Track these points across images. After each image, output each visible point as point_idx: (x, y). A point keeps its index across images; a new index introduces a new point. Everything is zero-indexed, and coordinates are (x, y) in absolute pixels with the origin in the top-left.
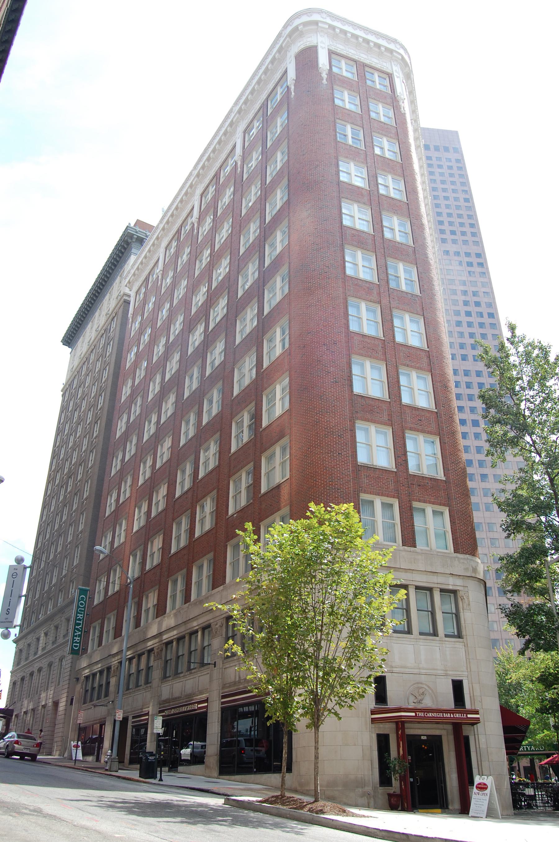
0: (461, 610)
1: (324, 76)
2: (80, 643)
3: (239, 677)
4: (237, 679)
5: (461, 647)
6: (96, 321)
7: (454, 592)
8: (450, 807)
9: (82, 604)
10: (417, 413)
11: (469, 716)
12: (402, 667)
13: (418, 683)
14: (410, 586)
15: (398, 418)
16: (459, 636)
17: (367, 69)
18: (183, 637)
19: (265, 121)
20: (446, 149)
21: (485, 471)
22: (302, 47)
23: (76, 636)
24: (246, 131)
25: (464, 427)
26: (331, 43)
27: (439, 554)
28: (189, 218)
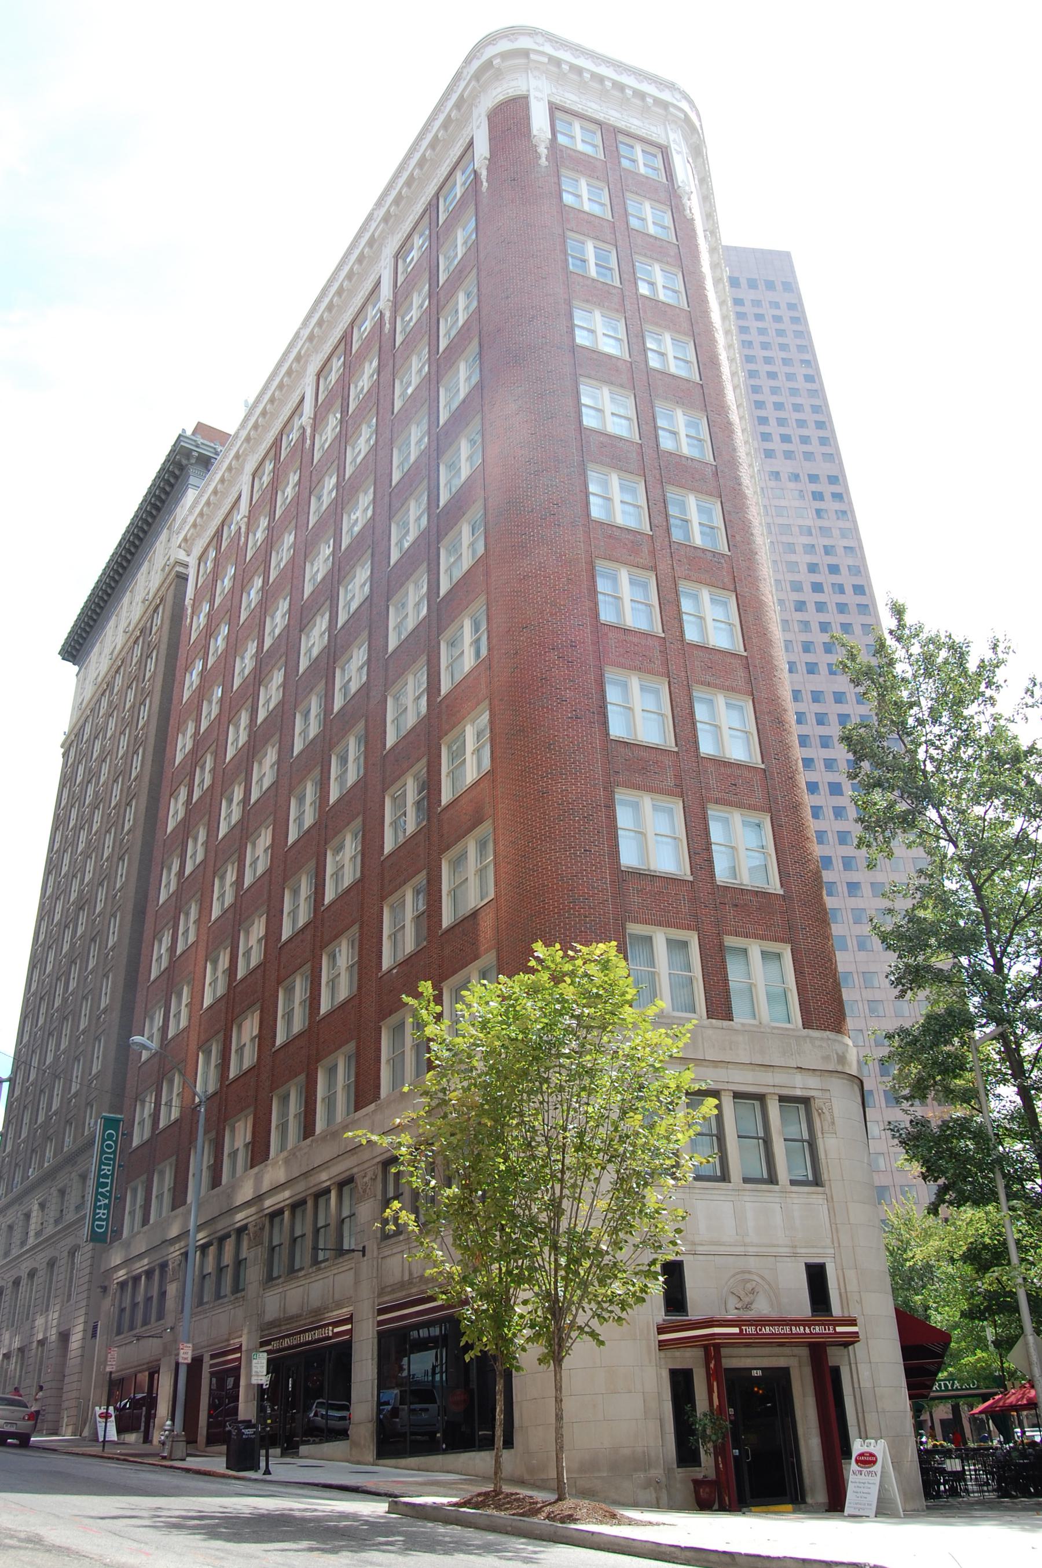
0: (819, 1135)
1: (543, 150)
2: (107, 1220)
3: (411, 1274)
4: (406, 1278)
5: (821, 1202)
6: (124, 613)
7: (806, 1101)
8: (809, 1500)
9: (109, 1146)
10: (729, 771)
11: (839, 1329)
13: (743, 1272)
14: (723, 1093)
15: (692, 781)
17: (621, 138)
18: (302, 1203)
19: (434, 236)
20: (770, 285)
21: (855, 877)
22: (501, 98)
23: (100, 1207)
24: (399, 255)
25: (815, 796)
26: (554, 90)
27: (775, 1031)
28: (296, 418)
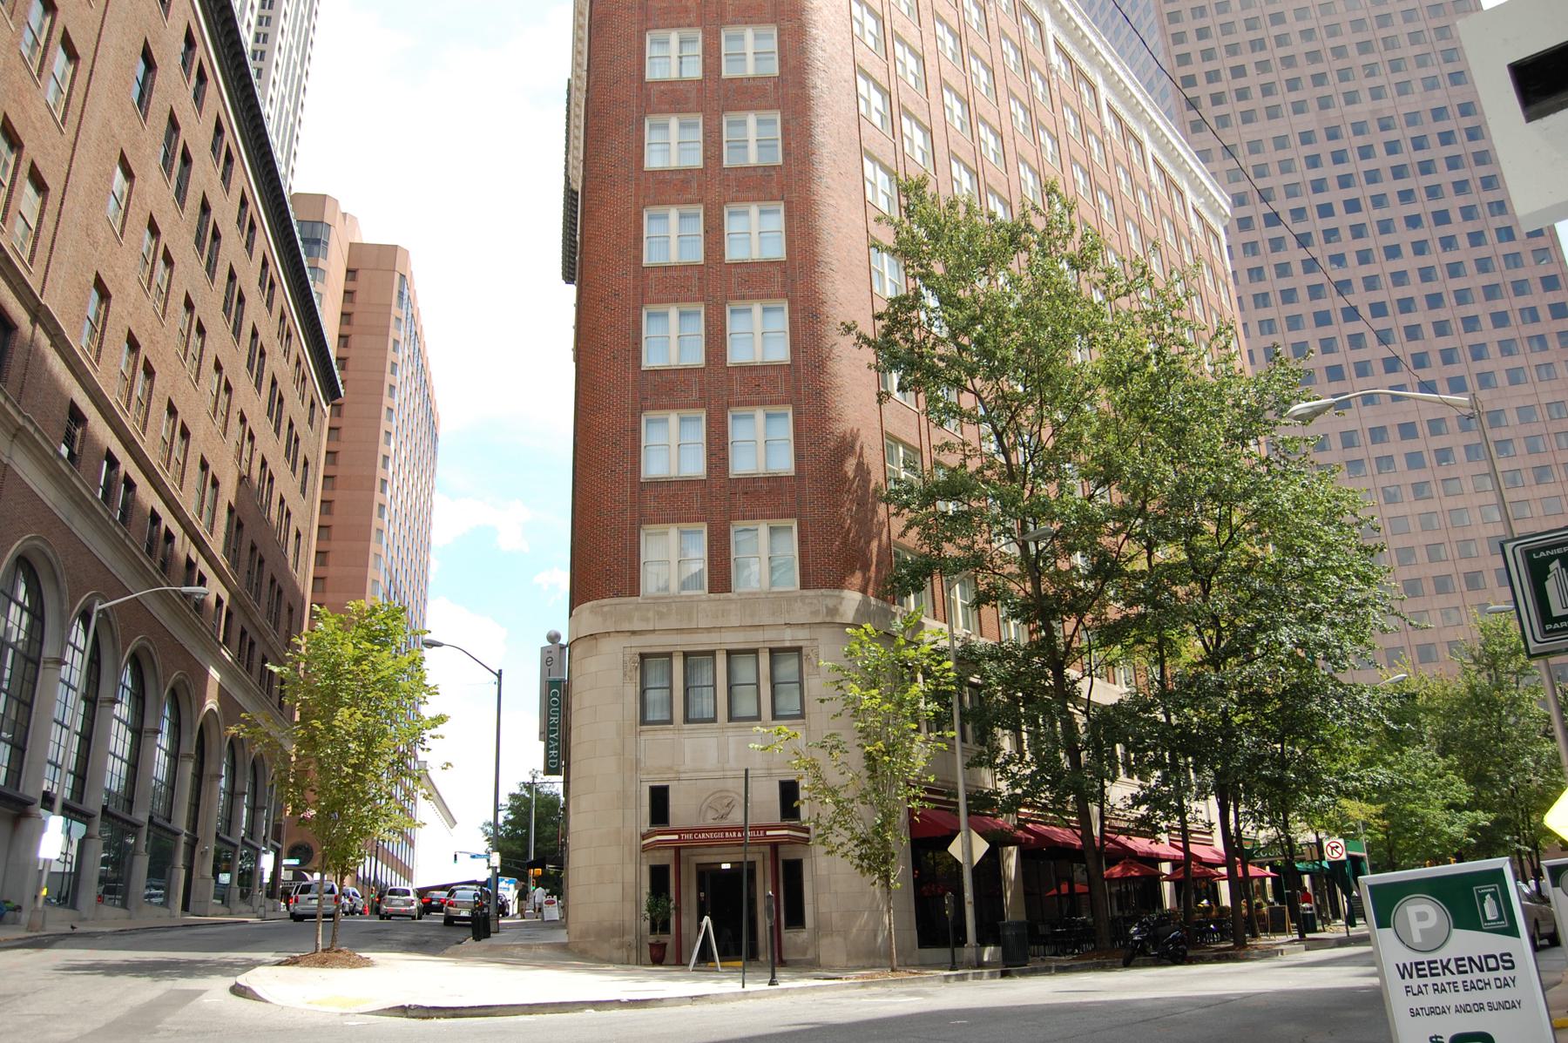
7: (799, 650)
8: (762, 958)
12: (695, 771)
16: (802, 716)
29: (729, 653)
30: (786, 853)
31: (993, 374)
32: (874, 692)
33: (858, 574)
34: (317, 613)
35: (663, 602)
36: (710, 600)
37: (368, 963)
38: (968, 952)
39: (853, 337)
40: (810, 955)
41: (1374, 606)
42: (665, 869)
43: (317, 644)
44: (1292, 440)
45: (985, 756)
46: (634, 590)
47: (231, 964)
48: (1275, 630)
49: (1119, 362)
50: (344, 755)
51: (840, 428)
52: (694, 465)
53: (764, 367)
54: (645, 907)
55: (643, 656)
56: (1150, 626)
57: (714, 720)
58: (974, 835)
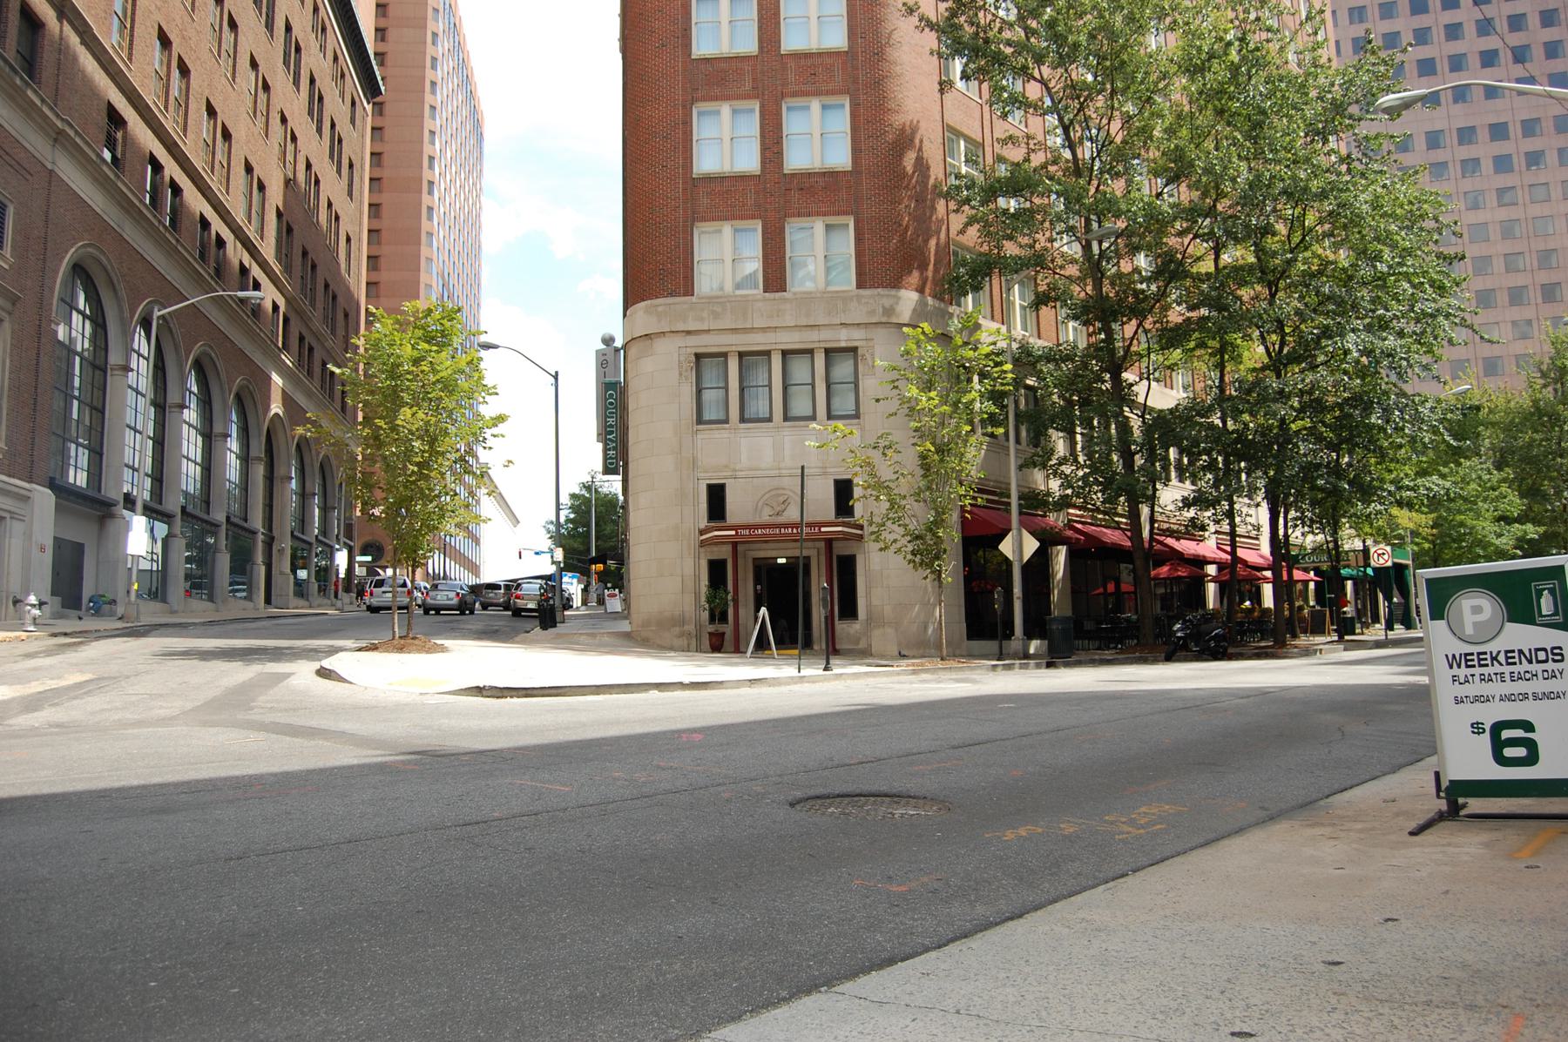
7: (854, 350)
8: (816, 647)
16: (857, 416)
29: (785, 353)
30: (840, 549)
31: (1063, 61)
32: (933, 394)
33: (916, 274)
34: (373, 315)
35: (718, 302)
36: (765, 300)
37: (443, 649)
38: (1015, 644)
39: (915, 20)
40: (862, 645)
41: (1447, 316)
42: (723, 562)
43: (376, 345)
44: (1376, 138)
45: (1039, 457)
46: (689, 290)
47: (315, 651)
48: (1342, 336)
49: (1199, 49)
50: (408, 453)
51: (898, 120)
52: (748, 160)
53: (820, 54)
54: (703, 599)
55: (698, 356)
56: (1214, 331)
57: (770, 420)
58: (1025, 533)
